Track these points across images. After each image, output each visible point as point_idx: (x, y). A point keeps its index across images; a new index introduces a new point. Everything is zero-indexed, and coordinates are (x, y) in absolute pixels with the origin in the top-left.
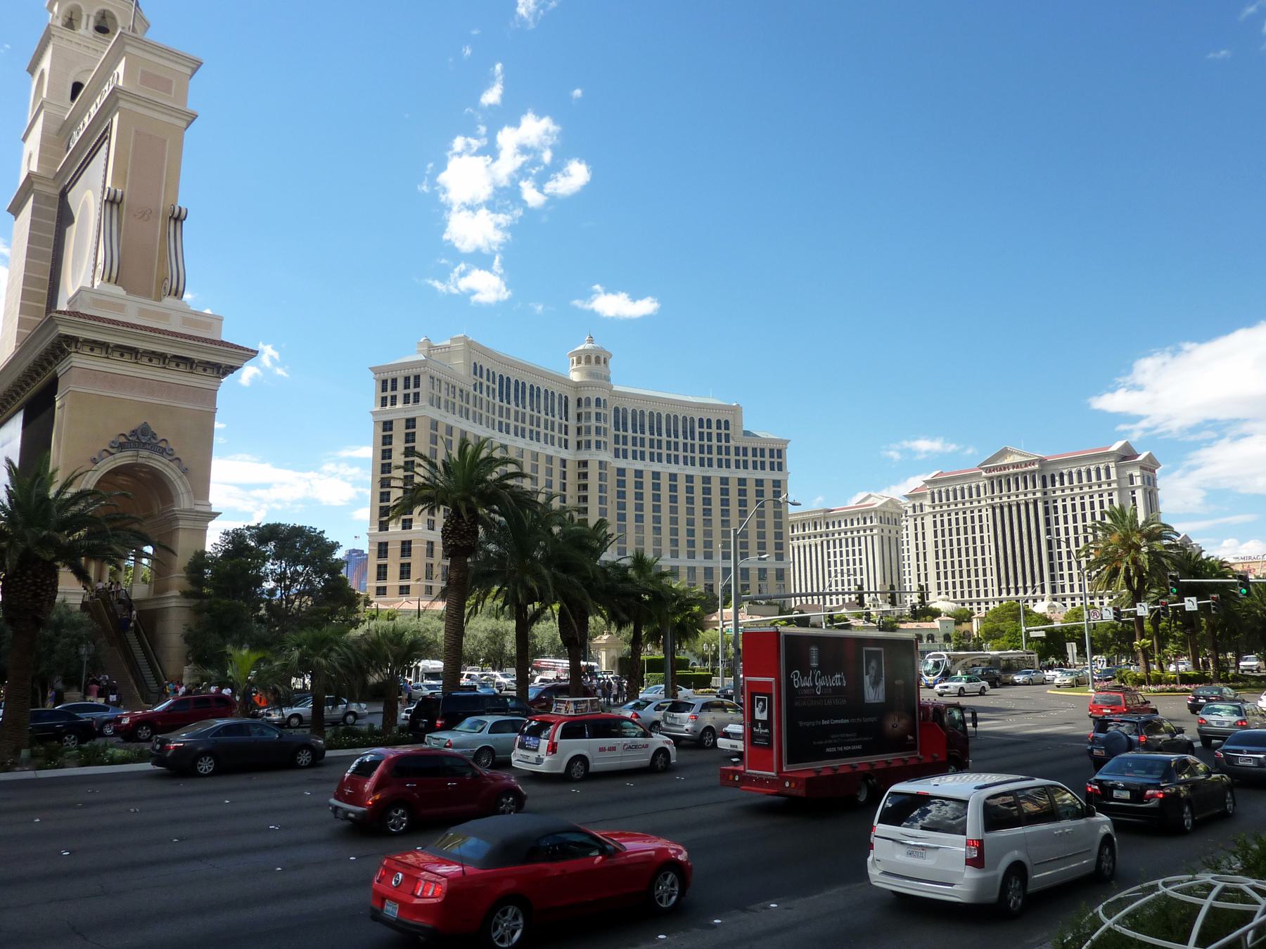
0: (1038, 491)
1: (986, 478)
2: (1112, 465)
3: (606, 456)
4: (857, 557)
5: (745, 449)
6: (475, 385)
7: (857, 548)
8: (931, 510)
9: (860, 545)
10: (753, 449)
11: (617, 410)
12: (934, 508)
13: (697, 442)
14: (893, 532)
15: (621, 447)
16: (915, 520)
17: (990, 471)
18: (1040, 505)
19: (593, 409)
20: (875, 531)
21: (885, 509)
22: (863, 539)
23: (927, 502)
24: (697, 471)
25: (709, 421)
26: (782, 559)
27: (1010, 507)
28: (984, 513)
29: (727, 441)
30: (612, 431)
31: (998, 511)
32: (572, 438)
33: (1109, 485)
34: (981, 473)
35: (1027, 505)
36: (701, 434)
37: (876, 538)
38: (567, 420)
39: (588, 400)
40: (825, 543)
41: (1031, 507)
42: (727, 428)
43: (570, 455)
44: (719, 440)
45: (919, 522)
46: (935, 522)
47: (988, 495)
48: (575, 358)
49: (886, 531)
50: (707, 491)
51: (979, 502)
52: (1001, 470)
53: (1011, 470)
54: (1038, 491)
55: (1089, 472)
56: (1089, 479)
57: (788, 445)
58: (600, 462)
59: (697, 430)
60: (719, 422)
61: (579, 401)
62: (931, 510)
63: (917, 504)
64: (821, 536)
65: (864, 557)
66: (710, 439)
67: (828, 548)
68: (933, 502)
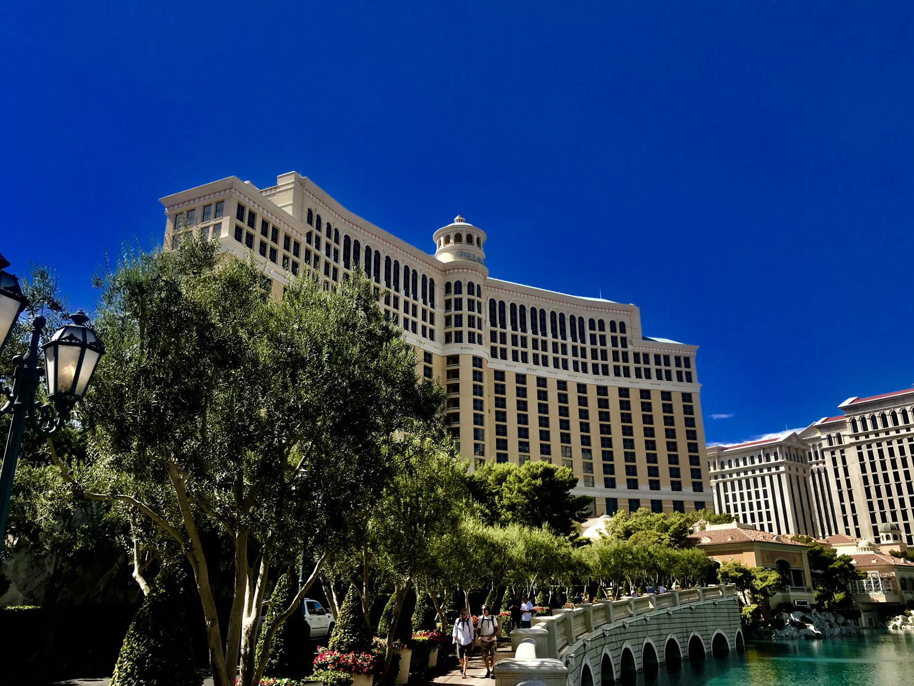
3: (483, 351)
4: (762, 500)
5: (646, 356)
6: (309, 235)
7: (760, 489)
8: (853, 440)
9: (764, 485)
10: (655, 356)
11: (492, 302)
12: (857, 438)
13: (588, 345)
14: (800, 470)
16: (833, 453)
19: (465, 296)
20: (782, 469)
21: (789, 444)
22: (767, 479)
23: (849, 431)
24: (591, 380)
25: (601, 322)
26: (701, 490)
29: (624, 345)
30: (487, 326)
32: (439, 328)
36: (593, 337)
37: (783, 477)
38: (433, 306)
39: (458, 285)
40: (721, 485)
42: (623, 330)
43: (437, 348)
44: (615, 344)
45: (838, 455)
46: (861, 456)
48: (442, 239)
49: (793, 469)
50: (603, 404)
58: (475, 358)
60: (613, 324)
61: (448, 285)
62: (853, 440)
63: (833, 435)
64: (716, 478)
65: (770, 499)
66: (603, 343)
67: (726, 490)
68: (855, 429)
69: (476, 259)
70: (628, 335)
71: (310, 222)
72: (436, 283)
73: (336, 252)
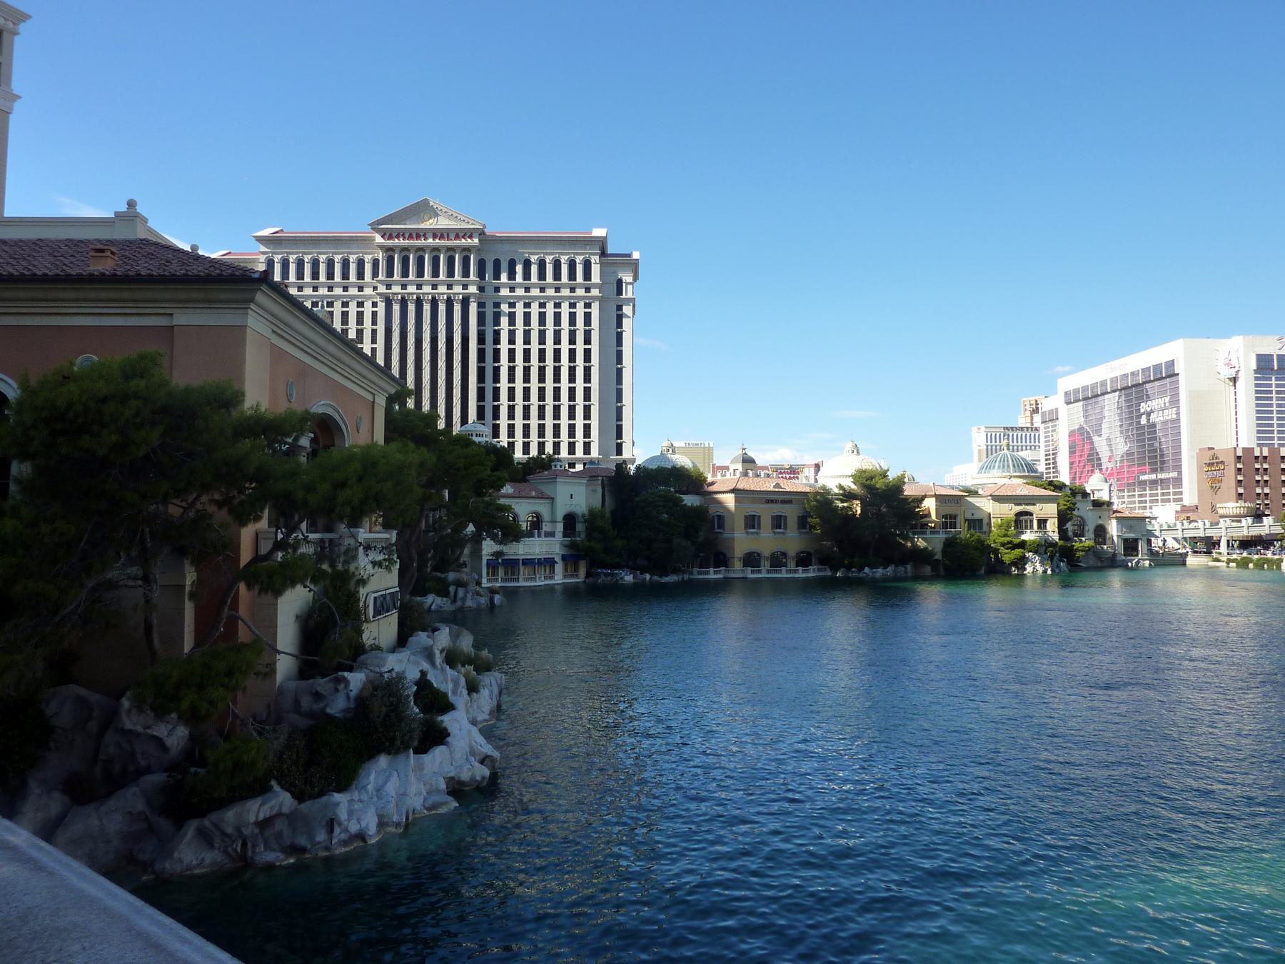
0: (473, 283)
1: (381, 247)
2: (595, 259)
17: (390, 237)
18: (473, 308)
27: (419, 303)
28: (368, 309)
31: (396, 308)
33: (588, 290)
34: (373, 239)
35: (449, 303)
47: (380, 277)
51: (361, 289)
52: (411, 237)
53: (430, 240)
54: (473, 283)
55: (557, 265)
56: (557, 276)
57: (22, 27)
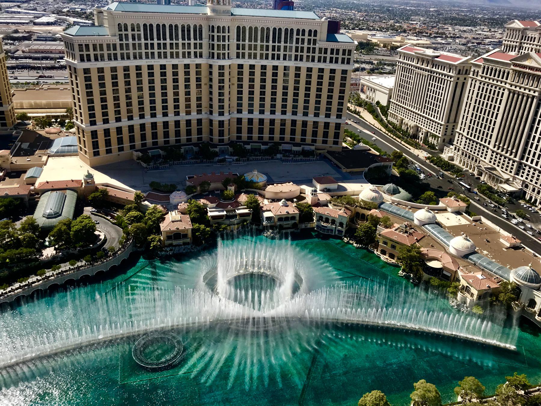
10: (331, 49)
11: (238, 27)
13: (294, 45)
15: (241, 51)
16: (472, 80)
20: (452, 79)
24: (292, 64)
25: (304, 31)
29: (315, 43)
30: (234, 42)
31: (511, 95)
32: (205, 50)
36: (297, 39)
41: (530, 100)
42: (315, 35)
59: (295, 36)
63: (476, 71)
65: (443, 92)
69: (222, 12)
70: (317, 38)
71: (120, 30)
72: (203, 26)
73: (139, 36)
